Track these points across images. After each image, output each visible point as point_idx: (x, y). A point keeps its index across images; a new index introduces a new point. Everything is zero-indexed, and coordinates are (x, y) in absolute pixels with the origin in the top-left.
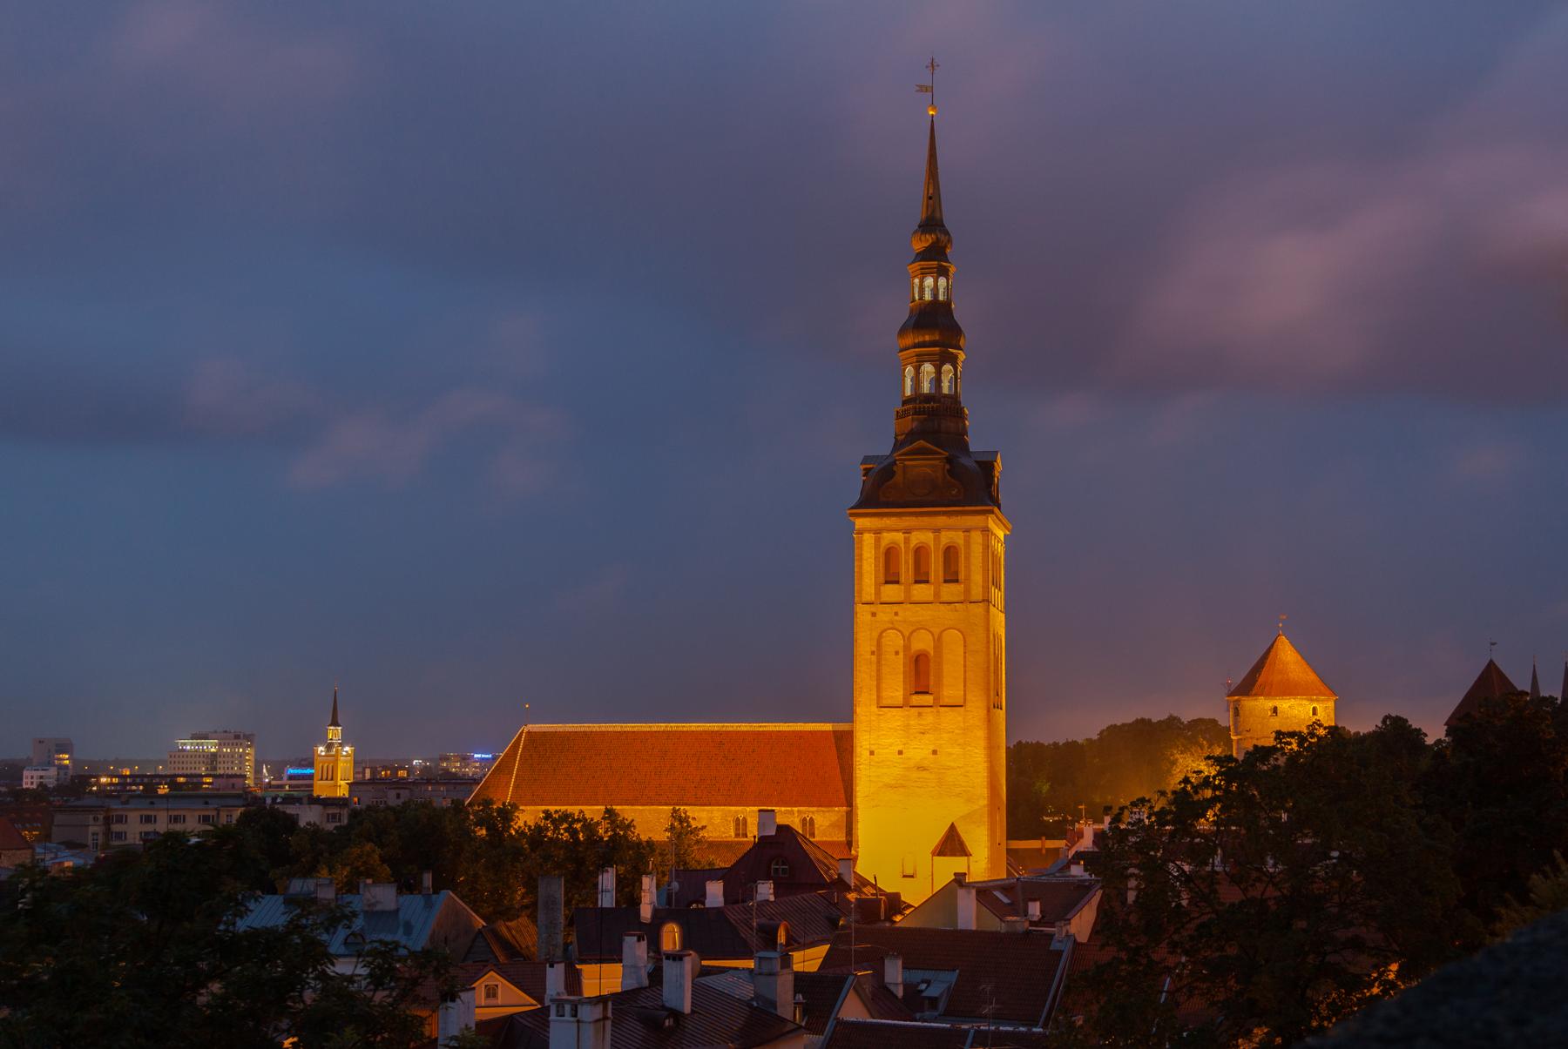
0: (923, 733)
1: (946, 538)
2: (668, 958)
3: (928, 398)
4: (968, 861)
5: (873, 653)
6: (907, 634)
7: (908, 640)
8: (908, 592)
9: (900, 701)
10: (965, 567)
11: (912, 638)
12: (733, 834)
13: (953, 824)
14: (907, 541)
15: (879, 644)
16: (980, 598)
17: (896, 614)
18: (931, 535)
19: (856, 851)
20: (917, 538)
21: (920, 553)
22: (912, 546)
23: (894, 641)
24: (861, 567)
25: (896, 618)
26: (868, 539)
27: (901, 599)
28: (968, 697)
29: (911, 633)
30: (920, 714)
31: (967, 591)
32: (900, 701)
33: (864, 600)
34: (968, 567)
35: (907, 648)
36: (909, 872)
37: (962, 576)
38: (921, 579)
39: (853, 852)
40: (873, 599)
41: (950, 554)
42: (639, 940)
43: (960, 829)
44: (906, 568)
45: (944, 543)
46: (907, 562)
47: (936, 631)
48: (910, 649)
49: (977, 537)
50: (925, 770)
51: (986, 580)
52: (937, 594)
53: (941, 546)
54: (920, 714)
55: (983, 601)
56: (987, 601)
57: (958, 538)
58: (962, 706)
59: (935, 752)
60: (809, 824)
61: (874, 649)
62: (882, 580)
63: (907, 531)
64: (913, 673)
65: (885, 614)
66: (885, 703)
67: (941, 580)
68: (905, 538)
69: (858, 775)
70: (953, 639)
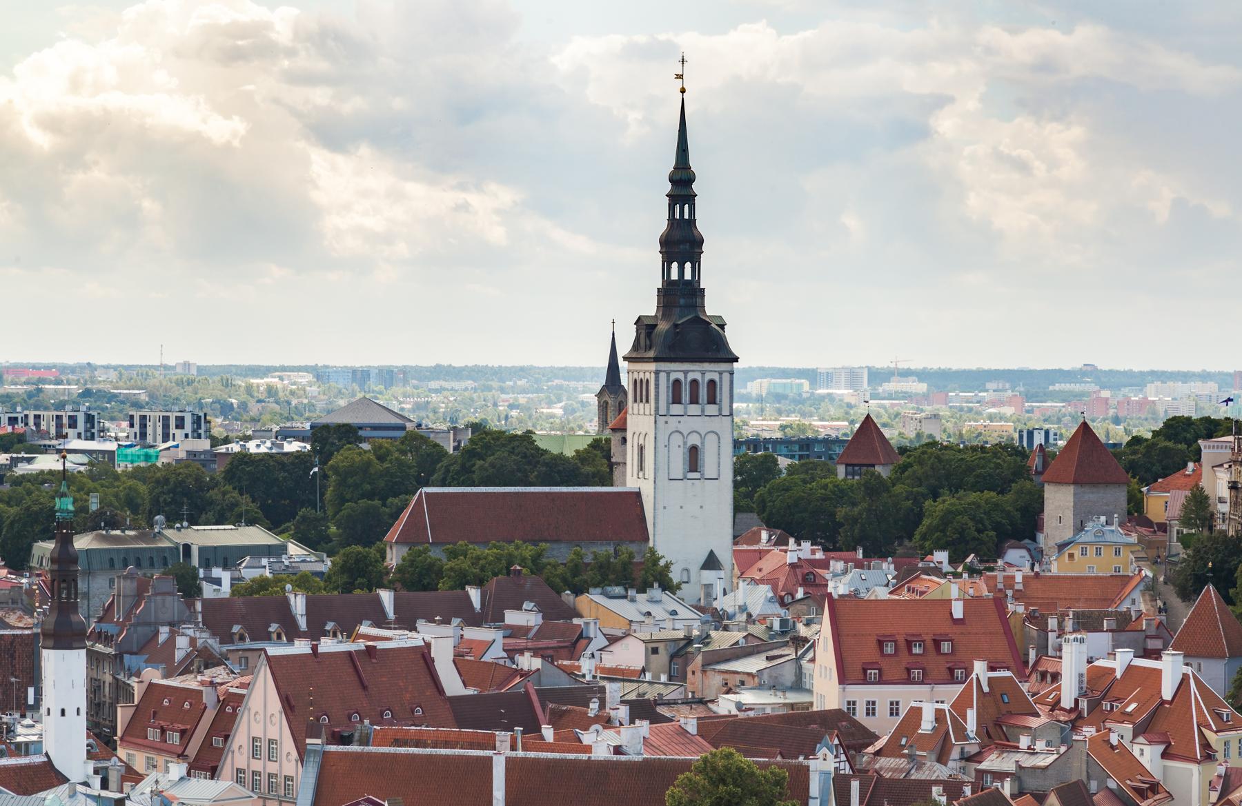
1: (708, 377)
5: (666, 446)
8: (685, 408)
11: (689, 437)
13: (712, 551)
14: (686, 378)
17: (680, 422)
23: (677, 440)
30: (693, 484)
31: (720, 410)
34: (721, 394)
35: (685, 443)
38: (694, 400)
44: (686, 396)
46: (686, 389)
49: (726, 377)
54: (693, 484)
57: (716, 377)
59: (701, 507)
61: (666, 444)
62: (670, 401)
67: (706, 402)
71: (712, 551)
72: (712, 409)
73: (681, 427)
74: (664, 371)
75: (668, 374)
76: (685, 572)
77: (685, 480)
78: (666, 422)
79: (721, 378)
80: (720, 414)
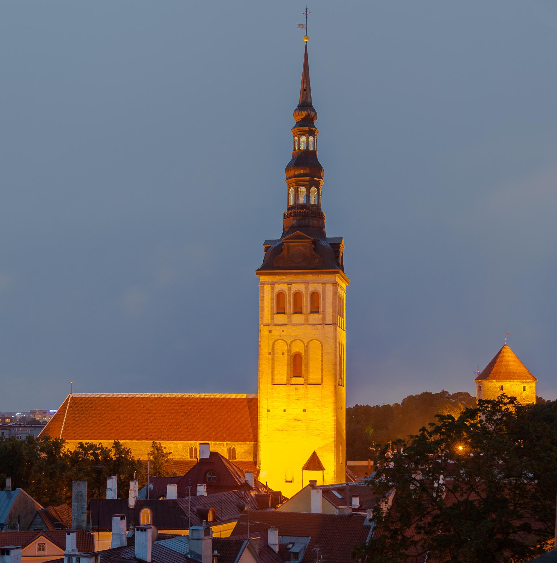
0: (298, 400)
1: (312, 288)
2: (138, 530)
3: (303, 207)
4: (323, 473)
5: (269, 353)
6: (289, 343)
7: (290, 346)
8: (289, 318)
9: (285, 382)
10: (323, 304)
12: (189, 457)
14: (289, 289)
15: (273, 349)
16: (331, 322)
17: (283, 331)
18: (303, 286)
19: (259, 467)
20: (295, 288)
21: (297, 296)
22: (292, 292)
23: (281, 347)
24: (263, 304)
25: (283, 333)
26: (267, 288)
27: (286, 323)
28: (324, 379)
29: (292, 342)
30: (296, 389)
31: (324, 318)
32: (285, 382)
33: (264, 323)
34: (324, 304)
35: (289, 351)
36: (288, 479)
37: (321, 310)
38: (298, 311)
39: (258, 468)
40: (270, 322)
41: (314, 296)
42: (121, 519)
43: (319, 455)
44: (289, 306)
45: (311, 291)
46: (289, 301)
47: (306, 341)
49: (329, 287)
50: (299, 421)
51: (334, 312)
52: (306, 320)
53: (309, 292)
54: (296, 389)
55: (333, 324)
56: (335, 324)
57: (319, 288)
58: (320, 384)
59: (304, 411)
60: (232, 452)
61: (270, 351)
62: (275, 311)
63: (290, 284)
64: (292, 365)
65: (277, 331)
66: (276, 382)
67: (309, 311)
68: (288, 287)
69: (260, 424)
70: (315, 346)
71: (314, 454)
72: (315, 318)
74: (268, 284)
78: (270, 331)
79: (324, 290)
80: (324, 323)
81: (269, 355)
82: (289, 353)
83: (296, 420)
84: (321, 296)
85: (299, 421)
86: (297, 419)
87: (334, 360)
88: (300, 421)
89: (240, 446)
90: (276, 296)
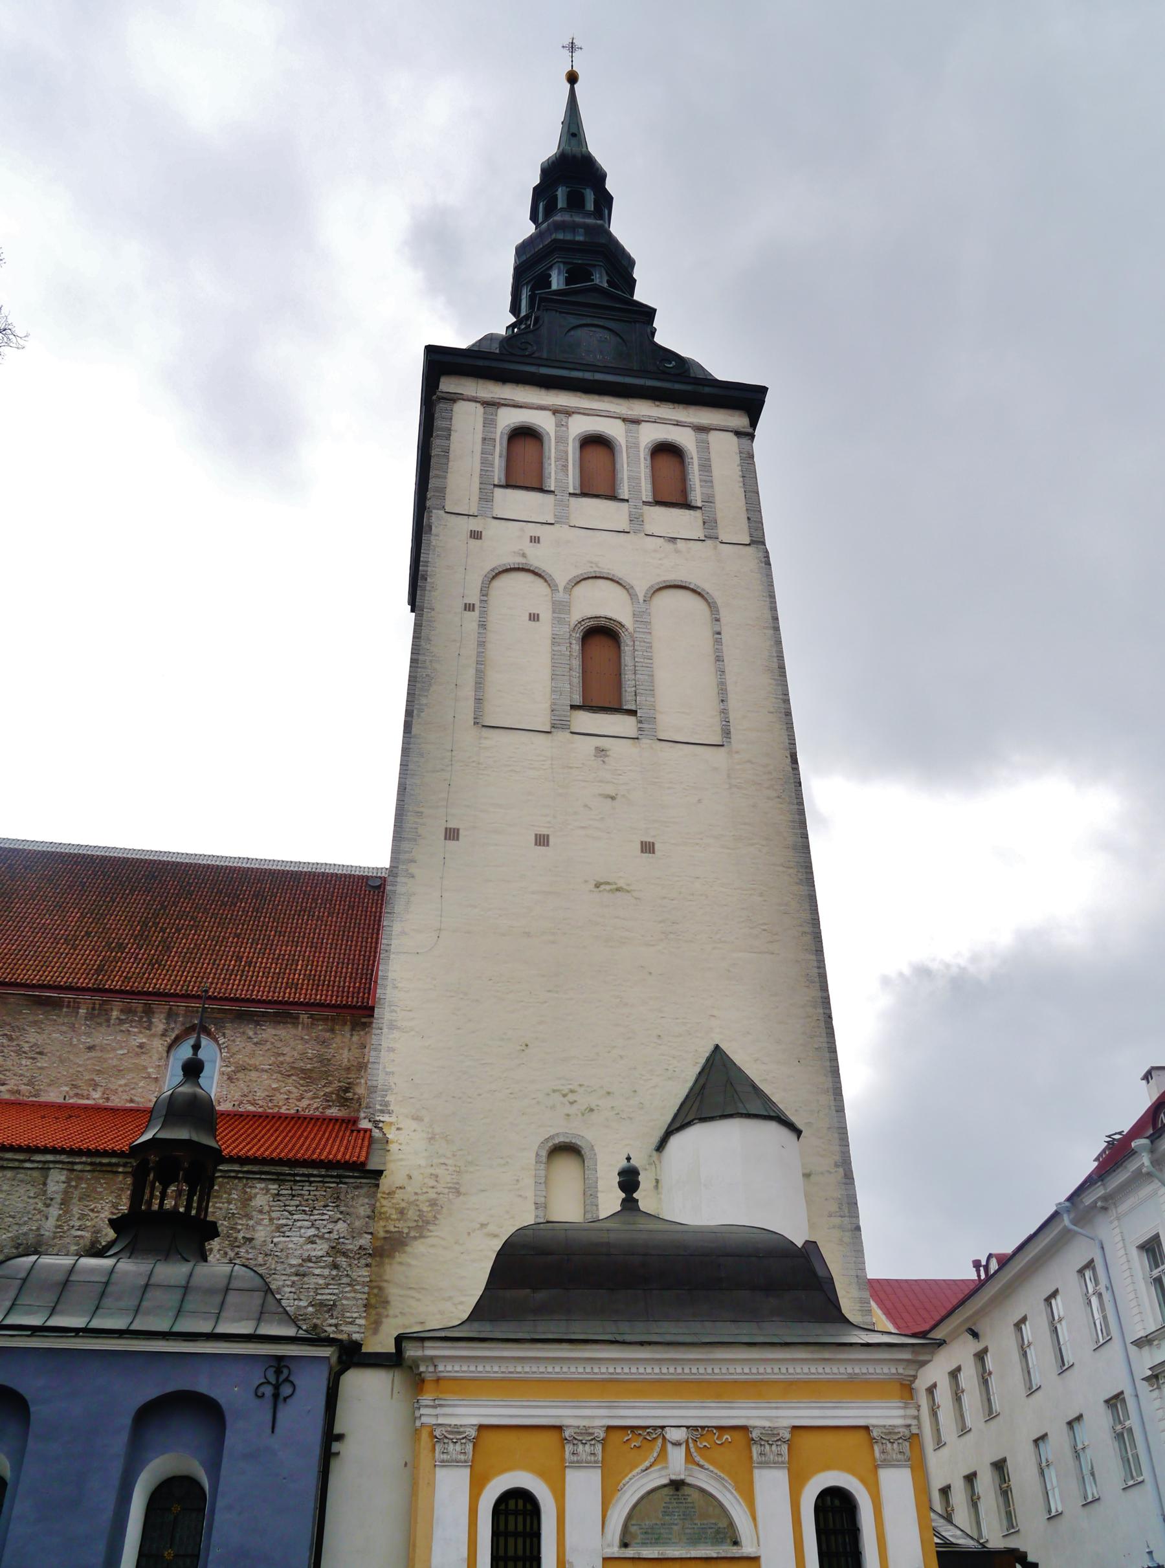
15: (485, 592)
30: (601, 752)
31: (710, 524)
35: (560, 608)
37: (696, 498)
48: (569, 612)
50: (618, 890)
52: (636, 520)
61: (474, 598)
62: (498, 473)
67: (646, 493)
73: (537, 557)
75: (491, 405)
76: (566, 1168)
77: (562, 736)
81: (468, 613)
82: (562, 616)
83: (602, 887)
84: (692, 458)
85: (618, 894)
86: (608, 883)
87: (775, 660)
88: (628, 892)
89: (251, 1033)
90: (506, 438)
